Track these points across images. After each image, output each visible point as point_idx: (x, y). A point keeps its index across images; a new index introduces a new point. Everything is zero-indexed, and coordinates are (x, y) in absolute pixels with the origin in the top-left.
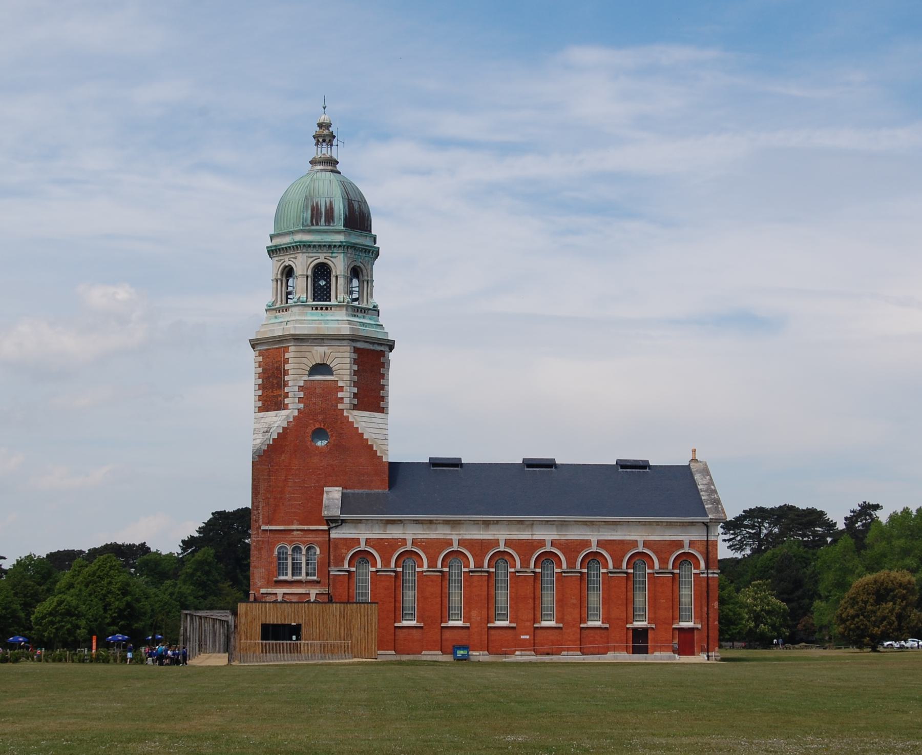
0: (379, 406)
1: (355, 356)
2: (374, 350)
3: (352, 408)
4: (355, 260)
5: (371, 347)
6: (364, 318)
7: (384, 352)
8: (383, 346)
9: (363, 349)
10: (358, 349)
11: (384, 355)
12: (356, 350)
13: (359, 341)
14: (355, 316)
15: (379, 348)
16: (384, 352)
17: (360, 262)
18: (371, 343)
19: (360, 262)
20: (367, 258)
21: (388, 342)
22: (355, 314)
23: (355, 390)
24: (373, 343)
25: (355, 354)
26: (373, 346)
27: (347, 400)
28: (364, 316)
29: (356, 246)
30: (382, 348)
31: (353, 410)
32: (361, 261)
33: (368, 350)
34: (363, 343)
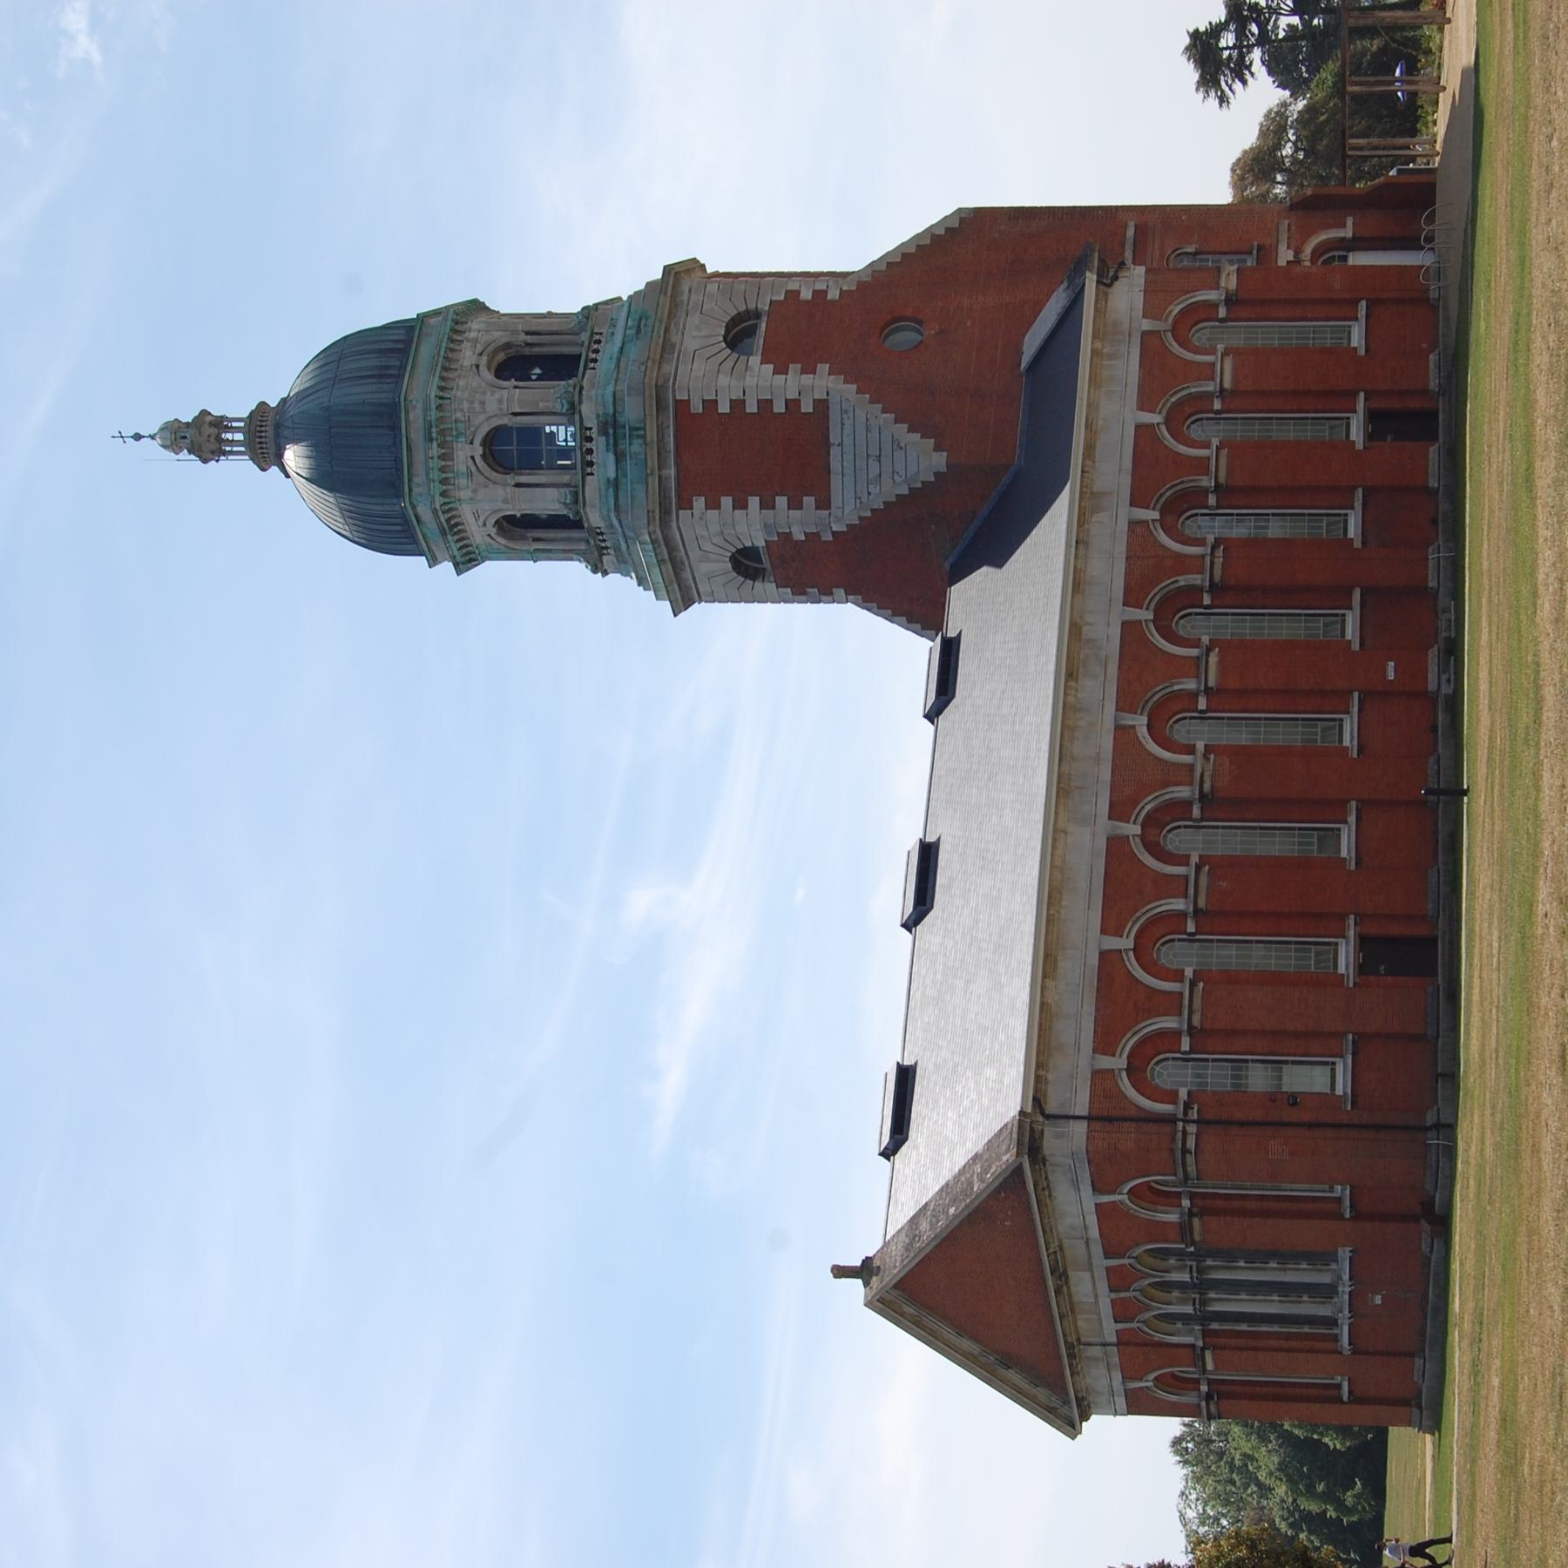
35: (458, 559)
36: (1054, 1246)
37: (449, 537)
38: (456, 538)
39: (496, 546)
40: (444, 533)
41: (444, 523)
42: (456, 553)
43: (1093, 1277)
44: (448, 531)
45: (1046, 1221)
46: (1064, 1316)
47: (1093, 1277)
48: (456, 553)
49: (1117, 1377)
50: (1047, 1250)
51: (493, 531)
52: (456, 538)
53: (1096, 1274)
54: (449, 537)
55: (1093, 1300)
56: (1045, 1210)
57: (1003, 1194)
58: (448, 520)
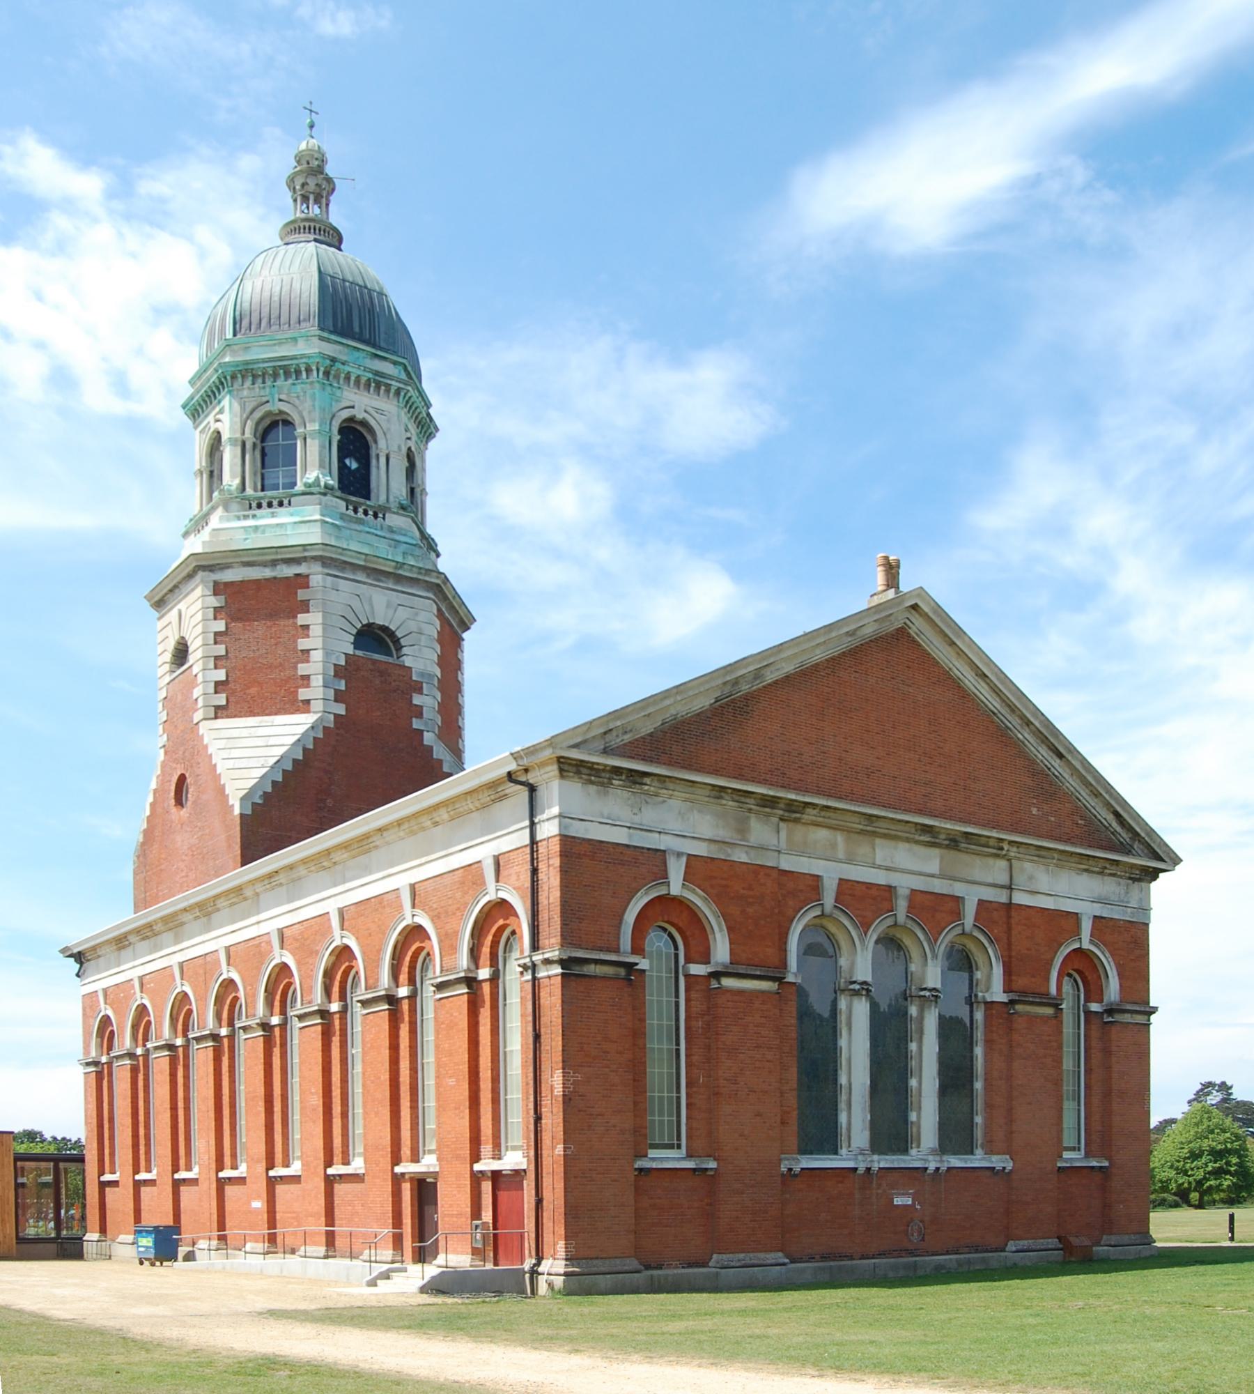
0: (296, 700)
1: (214, 602)
2: (275, 578)
3: (213, 716)
4: (265, 399)
5: (268, 573)
6: (273, 517)
7: (308, 576)
8: (304, 564)
9: (242, 581)
10: (228, 585)
11: (308, 583)
12: (218, 589)
13: (227, 566)
14: (246, 517)
15: (288, 571)
16: (308, 576)
17: (280, 400)
18: (264, 564)
19: (280, 400)
20: (298, 388)
21: (305, 550)
22: (246, 513)
23: (221, 675)
24: (274, 563)
25: (218, 597)
26: (273, 571)
27: (200, 703)
28: (273, 513)
29: (251, 367)
30: (302, 569)
31: (216, 718)
32: (283, 397)
33: (257, 584)
34: (261, 568)
35: (338, 365)
36: (1013, 852)
37: (370, 375)
38: (363, 380)
39: (336, 407)
40: (377, 373)
41: (389, 382)
42: (347, 368)
43: (933, 876)
44: (377, 378)
45: (1056, 855)
46: (872, 822)
47: (933, 876)
48: (347, 368)
49: (701, 850)
50: (1011, 843)
51: (360, 416)
52: (363, 380)
53: (936, 881)
54: (370, 375)
55: (878, 862)
56: (1073, 859)
57: (1080, 822)
58: (388, 387)
